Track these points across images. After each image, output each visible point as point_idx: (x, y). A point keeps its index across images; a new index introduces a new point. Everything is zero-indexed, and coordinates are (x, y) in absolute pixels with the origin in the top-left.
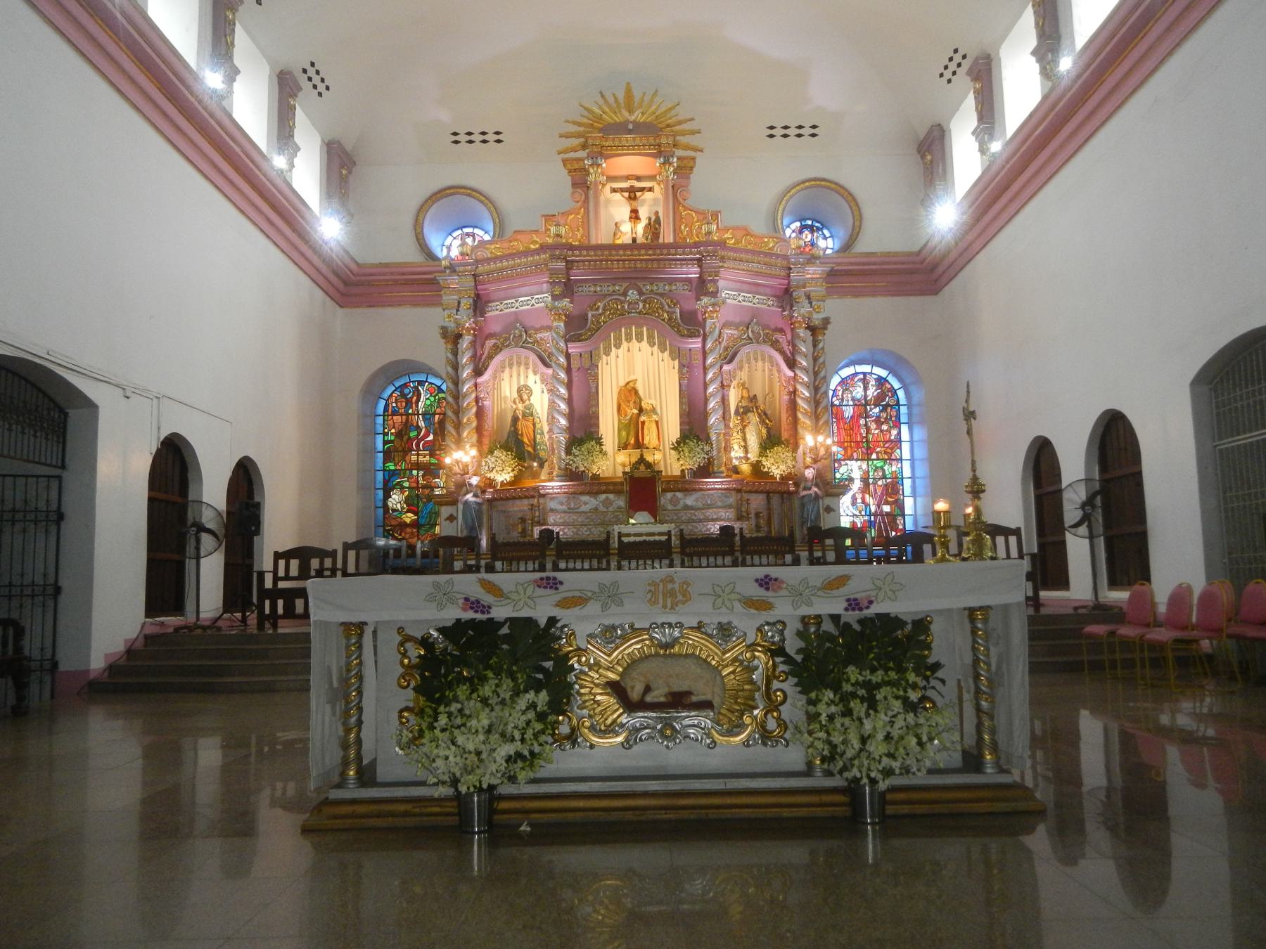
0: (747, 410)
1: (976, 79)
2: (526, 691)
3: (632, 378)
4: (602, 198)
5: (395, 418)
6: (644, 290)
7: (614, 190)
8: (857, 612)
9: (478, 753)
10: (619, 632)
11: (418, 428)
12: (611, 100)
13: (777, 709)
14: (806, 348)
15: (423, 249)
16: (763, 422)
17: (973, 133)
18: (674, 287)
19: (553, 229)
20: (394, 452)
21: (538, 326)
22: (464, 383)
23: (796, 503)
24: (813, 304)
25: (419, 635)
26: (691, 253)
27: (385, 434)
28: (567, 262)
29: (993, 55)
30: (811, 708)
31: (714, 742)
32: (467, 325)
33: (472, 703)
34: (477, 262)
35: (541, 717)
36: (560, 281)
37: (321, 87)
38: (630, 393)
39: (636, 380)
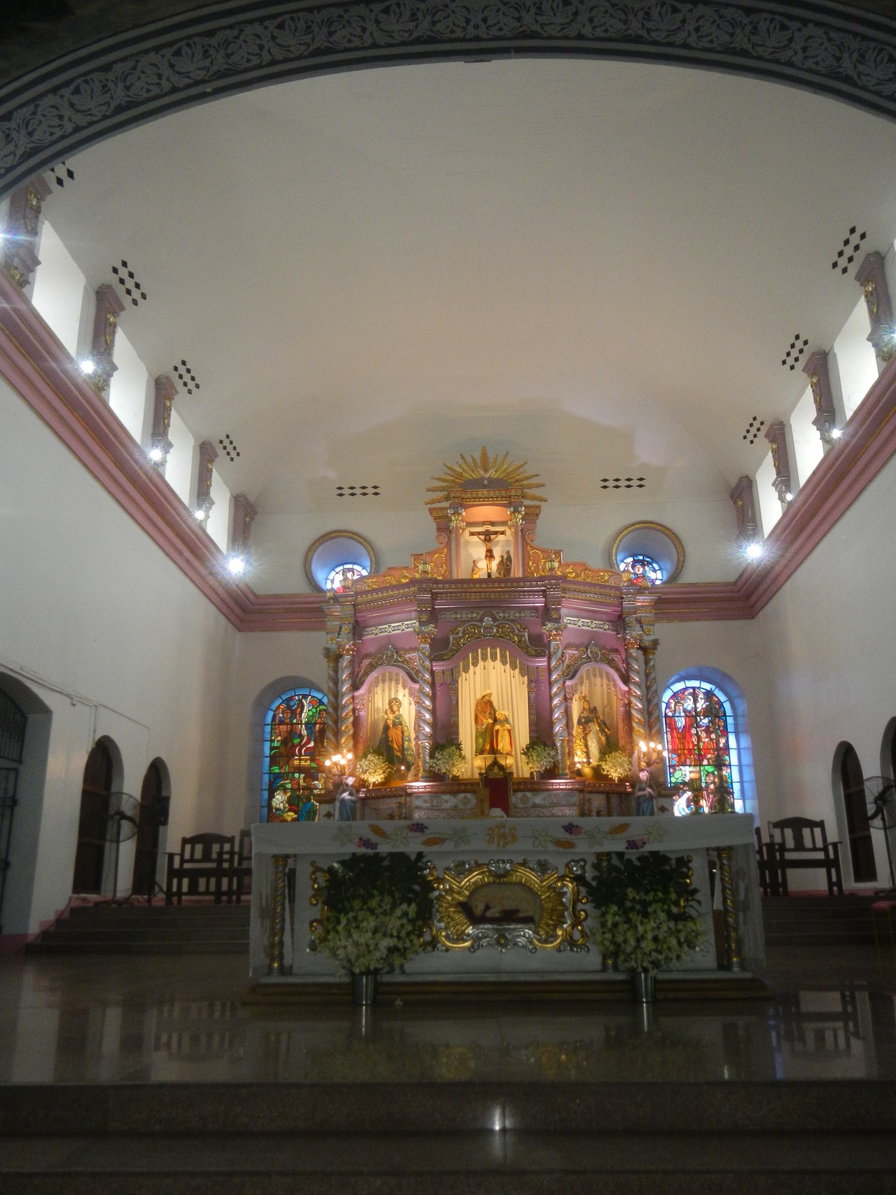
1: (772, 441)
2: (401, 903)
3: (488, 692)
4: (462, 540)
5: (281, 727)
6: (498, 617)
7: (472, 534)
8: (635, 850)
9: (368, 946)
10: (467, 866)
11: (301, 736)
12: (469, 460)
13: (580, 923)
14: (639, 667)
15: (311, 583)
16: (602, 731)
17: (773, 484)
18: (523, 615)
19: (421, 567)
20: (280, 757)
21: (407, 647)
22: (343, 695)
23: (633, 803)
24: (644, 627)
25: (326, 867)
26: (537, 586)
27: (272, 741)
28: (432, 594)
29: (785, 423)
30: (602, 919)
31: (535, 948)
32: (347, 647)
33: (363, 913)
34: (357, 594)
35: (412, 921)
36: (426, 610)
37: (233, 454)
38: (485, 706)
39: (491, 694)
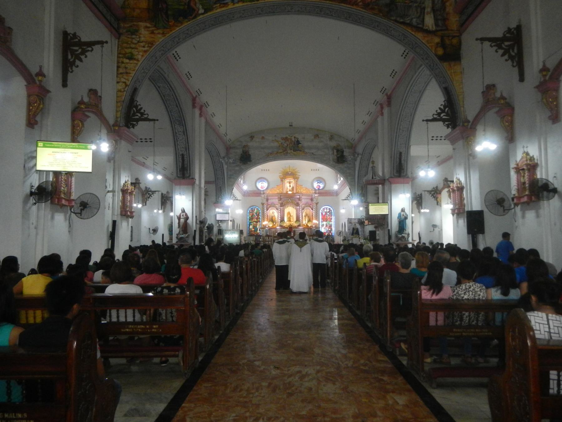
0: (306, 216)
38: (289, 213)
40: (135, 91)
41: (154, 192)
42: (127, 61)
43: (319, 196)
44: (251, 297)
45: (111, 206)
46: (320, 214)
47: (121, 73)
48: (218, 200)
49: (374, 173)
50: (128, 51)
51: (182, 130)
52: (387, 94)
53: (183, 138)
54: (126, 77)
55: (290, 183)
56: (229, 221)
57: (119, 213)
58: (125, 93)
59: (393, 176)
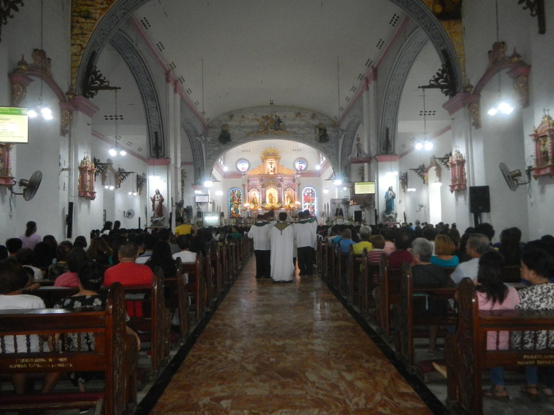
38: (271, 195)
40: (93, 56)
41: (128, 174)
42: (83, 20)
43: (301, 177)
44: (228, 288)
45: (67, 186)
46: (303, 195)
47: (76, 34)
48: (196, 182)
49: (360, 151)
50: (84, 8)
51: (155, 105)
52: (373, 67)
53: (156, 115)
54: (80, 38)
55: (271, 164)
56: (209, 203)
57: (77, 194)
58: (81, 57)
59: (379, 153)
